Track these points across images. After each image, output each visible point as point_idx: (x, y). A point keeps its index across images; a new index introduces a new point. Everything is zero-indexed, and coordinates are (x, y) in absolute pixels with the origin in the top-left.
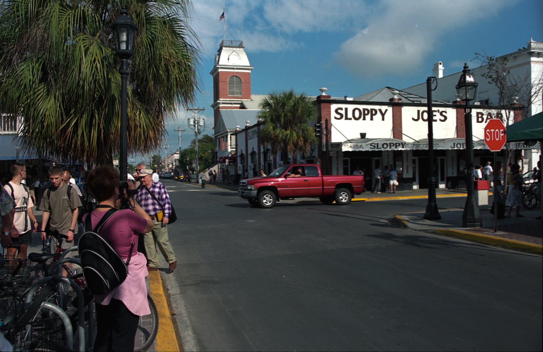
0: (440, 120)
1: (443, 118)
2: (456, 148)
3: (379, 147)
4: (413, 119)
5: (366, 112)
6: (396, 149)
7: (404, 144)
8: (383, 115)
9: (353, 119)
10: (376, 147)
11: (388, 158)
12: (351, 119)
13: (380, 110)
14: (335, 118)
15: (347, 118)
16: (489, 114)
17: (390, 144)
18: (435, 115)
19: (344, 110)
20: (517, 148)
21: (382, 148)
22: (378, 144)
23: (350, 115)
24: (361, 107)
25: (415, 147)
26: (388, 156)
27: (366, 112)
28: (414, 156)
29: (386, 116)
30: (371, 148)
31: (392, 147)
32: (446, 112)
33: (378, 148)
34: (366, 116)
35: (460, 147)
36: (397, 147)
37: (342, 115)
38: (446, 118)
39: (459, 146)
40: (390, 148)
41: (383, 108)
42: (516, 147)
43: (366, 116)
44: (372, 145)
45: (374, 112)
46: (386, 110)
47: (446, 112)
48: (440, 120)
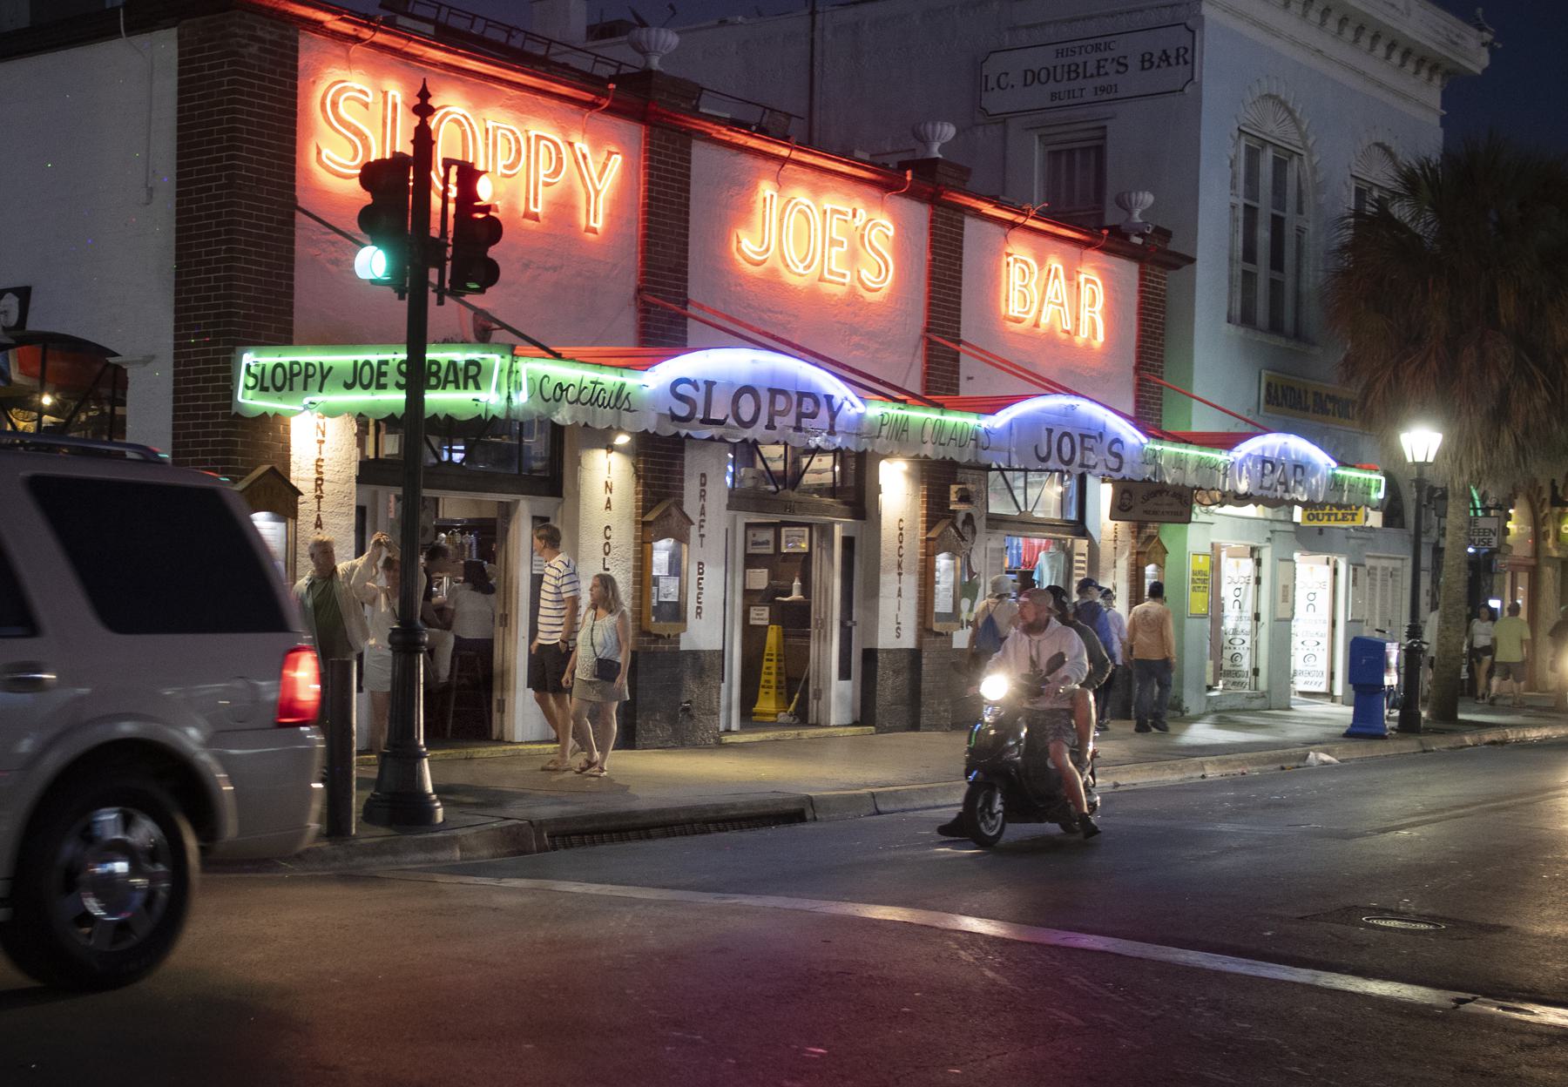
33: (707, 421)
36: (805, 422)
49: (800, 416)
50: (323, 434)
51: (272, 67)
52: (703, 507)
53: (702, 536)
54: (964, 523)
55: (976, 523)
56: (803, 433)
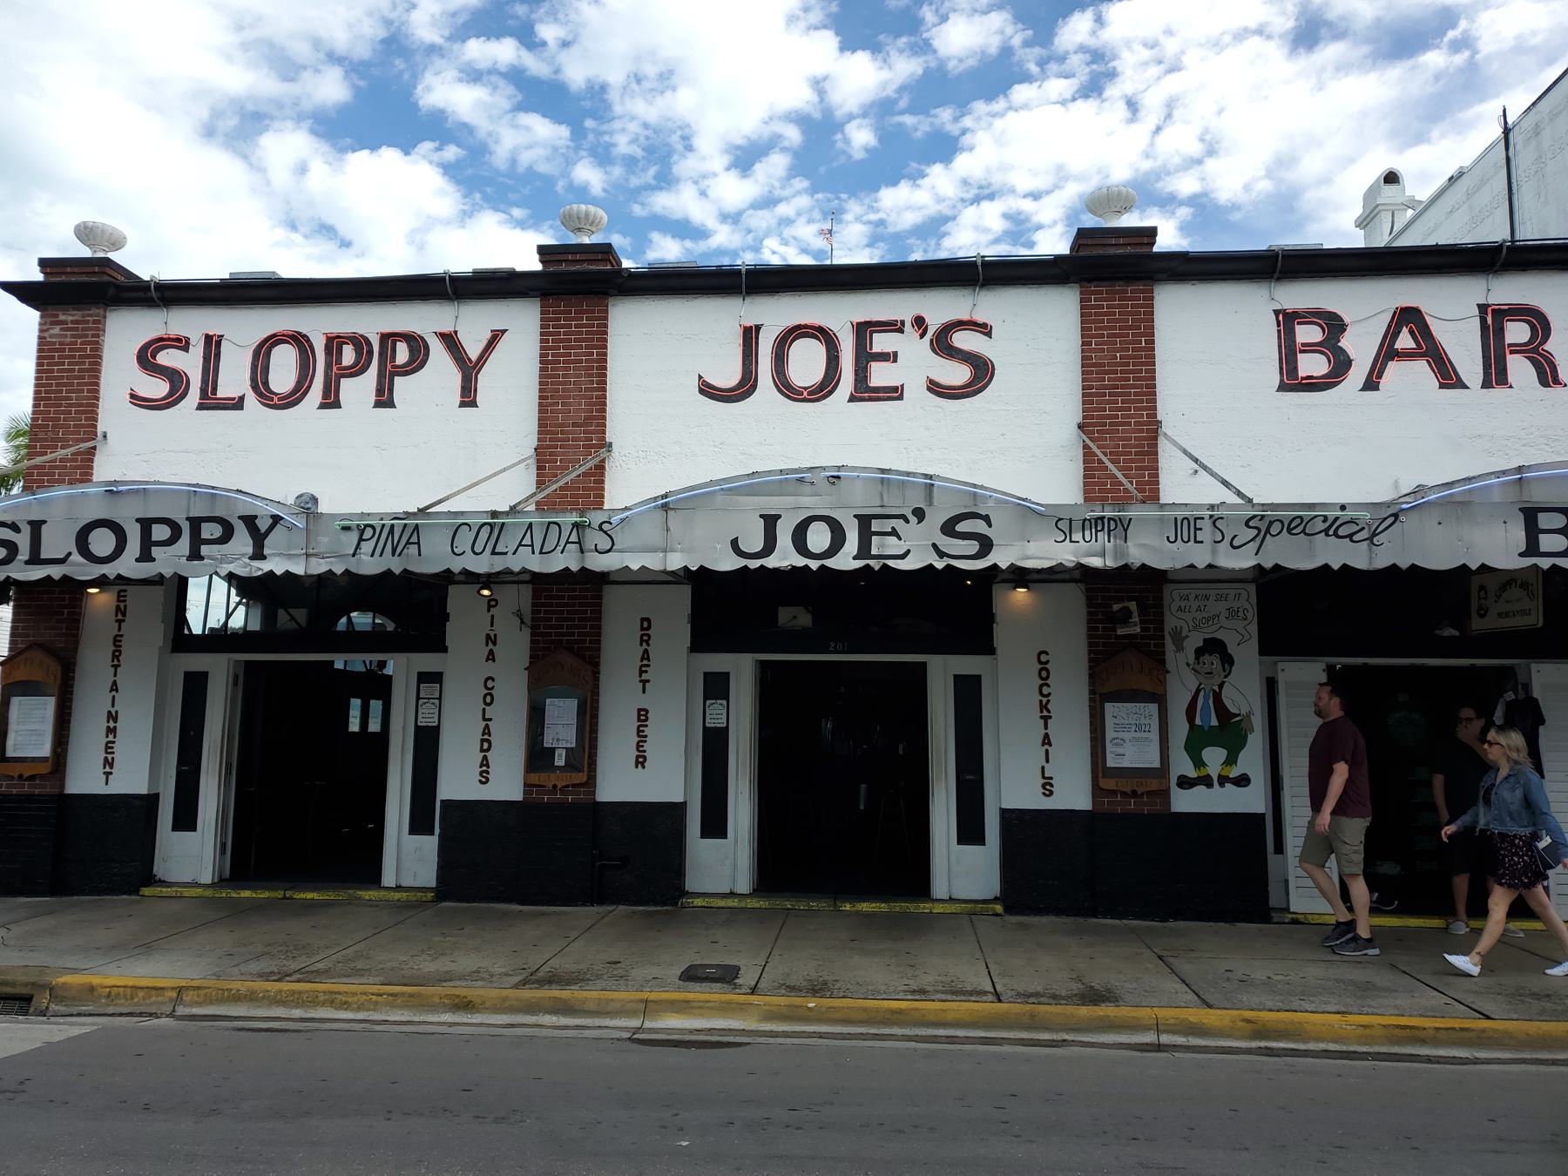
1: (958, 374)
2: (785, 557)
4: (708, 390)
5: (348, 356)
7: (263, 525)
8: (469, 371)
9: (251, 400)
10: (24, 554)
11: (491, 656)
12: (237, 404)
13: (451, 341)
14: (135, 398)
15: (210, 401)
17: (146, 524)
18: (891, 357)
21: (76, 557)
22: (36, 526)
23: (234, 377)
24: (318, 323)
25: (367, 547)
26: (491, 639)
27: (348, 356)
29: (485, 380)
31: (156, 551)
32: (985, 329)
33: (35, 559)
35: (833, 550)
36: (205, 550)
37: (176, 379)
39: (819, 538)
40: (145, 556)
45: (402, 354)
46: (496, 336)
47: (985, 329)
48: (935, 388)
49: (197, 542)
50: (124, 614)
52: (646, 651)
53: (645, 682)
54: (1199, 652)
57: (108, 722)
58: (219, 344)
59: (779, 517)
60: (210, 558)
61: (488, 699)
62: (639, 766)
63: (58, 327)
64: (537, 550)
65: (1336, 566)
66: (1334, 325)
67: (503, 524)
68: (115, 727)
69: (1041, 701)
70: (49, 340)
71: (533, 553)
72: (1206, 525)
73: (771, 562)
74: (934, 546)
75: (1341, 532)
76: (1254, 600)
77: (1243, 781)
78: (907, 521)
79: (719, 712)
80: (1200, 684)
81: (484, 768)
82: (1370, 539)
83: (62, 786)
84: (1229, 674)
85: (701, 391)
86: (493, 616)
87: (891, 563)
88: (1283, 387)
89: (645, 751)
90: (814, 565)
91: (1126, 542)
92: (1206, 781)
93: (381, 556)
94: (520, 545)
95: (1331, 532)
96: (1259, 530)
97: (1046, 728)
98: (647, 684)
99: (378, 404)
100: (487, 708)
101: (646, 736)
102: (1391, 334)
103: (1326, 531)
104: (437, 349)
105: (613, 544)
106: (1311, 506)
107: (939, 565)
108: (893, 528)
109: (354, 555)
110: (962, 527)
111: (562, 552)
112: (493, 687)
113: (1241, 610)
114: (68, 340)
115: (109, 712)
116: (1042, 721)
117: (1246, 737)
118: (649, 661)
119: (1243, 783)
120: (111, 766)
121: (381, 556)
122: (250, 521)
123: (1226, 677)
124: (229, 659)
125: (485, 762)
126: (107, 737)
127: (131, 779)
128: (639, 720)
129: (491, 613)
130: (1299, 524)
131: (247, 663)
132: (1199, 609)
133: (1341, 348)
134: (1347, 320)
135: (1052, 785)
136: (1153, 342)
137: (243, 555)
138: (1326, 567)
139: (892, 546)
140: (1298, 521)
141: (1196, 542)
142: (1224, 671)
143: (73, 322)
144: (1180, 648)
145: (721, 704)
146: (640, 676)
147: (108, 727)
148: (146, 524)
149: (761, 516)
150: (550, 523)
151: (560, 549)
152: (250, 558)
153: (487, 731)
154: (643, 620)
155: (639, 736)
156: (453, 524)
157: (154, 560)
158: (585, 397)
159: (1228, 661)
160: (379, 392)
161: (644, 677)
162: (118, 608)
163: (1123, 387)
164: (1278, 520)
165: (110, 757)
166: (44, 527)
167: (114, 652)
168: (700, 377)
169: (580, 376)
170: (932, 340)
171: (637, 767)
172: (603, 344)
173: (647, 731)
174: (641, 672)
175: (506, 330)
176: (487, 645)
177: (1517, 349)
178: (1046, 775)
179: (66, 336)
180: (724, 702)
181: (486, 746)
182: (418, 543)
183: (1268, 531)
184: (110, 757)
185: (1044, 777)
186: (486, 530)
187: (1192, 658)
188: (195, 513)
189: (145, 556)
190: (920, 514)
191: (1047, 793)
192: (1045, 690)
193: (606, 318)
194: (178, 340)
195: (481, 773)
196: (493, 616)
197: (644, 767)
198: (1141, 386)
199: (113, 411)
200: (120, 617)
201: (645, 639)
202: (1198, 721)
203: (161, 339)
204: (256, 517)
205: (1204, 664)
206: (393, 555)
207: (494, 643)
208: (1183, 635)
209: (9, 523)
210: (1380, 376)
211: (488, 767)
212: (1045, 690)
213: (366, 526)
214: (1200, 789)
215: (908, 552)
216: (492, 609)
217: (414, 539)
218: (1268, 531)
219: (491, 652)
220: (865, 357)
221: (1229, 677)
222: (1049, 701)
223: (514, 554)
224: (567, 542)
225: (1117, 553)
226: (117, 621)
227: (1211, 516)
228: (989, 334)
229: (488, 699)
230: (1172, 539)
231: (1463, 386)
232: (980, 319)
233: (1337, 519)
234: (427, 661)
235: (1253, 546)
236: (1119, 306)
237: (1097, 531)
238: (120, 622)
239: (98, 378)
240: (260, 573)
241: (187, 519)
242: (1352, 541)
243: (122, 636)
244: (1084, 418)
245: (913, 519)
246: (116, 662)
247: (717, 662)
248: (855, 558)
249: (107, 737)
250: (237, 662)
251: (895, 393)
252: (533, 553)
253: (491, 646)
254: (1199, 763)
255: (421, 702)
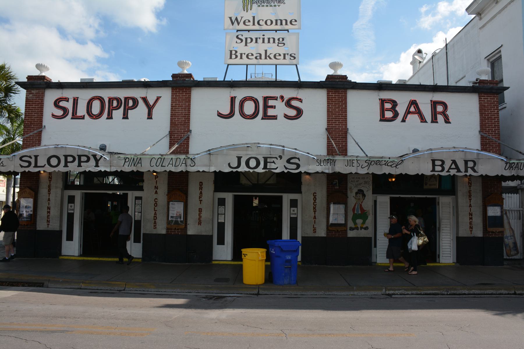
0: (286, 117)
1: (293, 113)
2: (243, 168)
3: (38, 165)
4: (220, 115)
5: (115, 103)
6: (81, 170)
7: (98, 158)
8: (150, 108)
9: (87, 117)
11: (156, 193)
12: (83, 118)
13: (145, 100)
14: (54, 116)
15: (75, 116)
16: (413, 103)
17: (66, 157)
18: (273, 107)
19: (71, 101)
20: (436, 174)
21: (47, 166)
22: (36, 157)
23: (82, 110)
24: (106, 94)
25: (127, 164)
26: (156, 188)
27: (115, 103)
28: (217, 189)
30: (22, 166)
32: (300, 100)
33: (36, 166)
34: (114, 112)
37: (65, 110)
38: (299, 112)
39: (253, 163)
40: (66, 166)
41: (151, 94)
42: (433, 170)
43: (114, 112)
44: (24, 159)
45: (131, 103)
46: (158, 98)
47: (300, 100)
48: (286, 117)
49: (80, 162)
50: (51, 179)
51: (36, 98)
52: (201, 192)
53: (201, 201)
54: (356, 193)
55: (365, 193)
56: (83, 167)
57: (48, 210)
58: (77, 100)
59: (242, 157)
60: (84, 166)
61: (156, 205)
62: (199, 225)
63: (31, 95)
64: (174, 165)
65: (387, 173)
66: (394, 104)
67: (164, 158)
68: (50, 211)
69: (314, 207)
70: (29, 98)
71: (173, 166)
72: (355, 162)
73: (239, 170)
74: (284, 166)
75: (389, 165)
76: (371, 179)
77: (366, 228)
78: (277, 159)
79: (223, 209)
80: (356, 202)
81: (155, 224)
82: (396, 166)
83: (36, 227)
84: (364, 199)
85: (218, 115)
86: (157, 181)
87: (273, 171)
88: (381, 120)
89: (201, 220)
90: (251, 171)
91: (335, 166)
92: (357, 228)
93: (131, 166)
94: (169, 164)
95: (386, 164)
96: (369, 163)
97: (315, 214)
98: (201, 201)
99: (124, 118)
100: (156, 208)
101: (201, 216)
102: (409, 107)
103: (385, 164)
104: (141, 102)
105: (195, 164)
106: (382, 157)
107: (286, 171)
108: (273, 161)
109: (123, 166)
110: (292, 161)
111: (181, 166)
112: (157, 201)
113: (368, 182)
114: (34, 98)
115: (48, 207)
116: (314, 212)
117: (368, 216)
118: (202, 194)
119: (367, 229)
120: (49, 222)
121: (131, 166)
122: (94, 156)
123: (363, 200)
124: (81, 192)
125: (155, 223)
126: (48, 214)
127: (54, 226)
128: (199, 212)
129: (156, 180)
130: (378, 163)
131: (85, 193)
132: (357, 181)
133: (396, 110)
134: (398, 103)
135: (316, 230)
136: (346, 106)
137: (93, 166)
138: (385, 173)
139: (273, 166)
140: (378, 161)
141: (353, 166)
142: (363, 198)
143: (36, 93)
144: (351, 192)
145: (223, 207)
146: (200, 199)
147: (48, 211)
148: (66, 157)
149: (237, 157)
150: (177, 158)
151: (180, 165)
152: (95, 167)
153: (155, 214)
154: (200, 182)
155: (199, 216)
156: (151, 158)
157: (68, 167)
158: (184, 117)
159: (364, 196)
160: (124, 114)
161: (201, 199)
162: (49, 177)
163: (338, 118)
164: (373, 161)
165: (49, 219)
166: (38, 157)
167: (49, 190)
168: (218, 111)
169: (183, 110)
170: (285, 103)
171: (199, 225)
172: (189, 101)
173: (202, 215)
174: (200, 198)
175: (161, 97)
176: (155, 189)
177: (440, 113)
178: (314, 227)
179: (33, 97)
180: (224, 207)
181: (155, 218)
182: (141, 163)
183: (371, 164)
184: (49, 219)
185: (314, 228)
186: (160, 159)
187: (354, 195)
188: (79, 154)
189: (66, 166)
190: (281, 157)
191: (315, 232)
192: (315, 204)
193: (190, 94)
194: (66, 98)
195: (154, 226)
196: (157, 181)
197: (201, 225)
198: (343, 119)
199: (47, 120)
200: (50, 179)
201: (201, 188)
202: (356, 212)
203: (61, 98)
204: (96, 155)
205: (358, 196)
206: (134, 166)
207: (157, 189)
208: (352, 188)
209: (29, 156)
210: (406, 118)
211: (156, 224)
212: (315, 204)
213: (127, 158)
214: (355, 231)
215: (277, 167)
216: (156, 179)
217: (140, 162)
218: (371, 164)
219: (156, 191)
220: (266, 107)
221: (364, 200)
222: (316, 207)
223: (167, 166)
224: (182, 163)
225: (332, 169)
226: (49, 181)
227: (357, 160)
228: (302, 102)
229: (156, 205)
230: (346, 165)
231: (426, 122)
232: (299, 97)
233: (388, 161)
234: (138, 194)
235: (367, 168)
236: (337, 96)
237: (327, 163)
238: (50, 181)
239: (43, 110)
240: (97, 171)
241: (78, 155)
242: (391, 167)
243: (51, 185)
244: (328, 127)
245: (279, 159)
246: (49, 193)
247: (222, 195)
248: (263, 169)
249: (48, 214)
250: (83, 193)
251: (274, 118)
252: (173, 166)
253: (156, 189)
254: (355, 223)
255: (136, 205)
